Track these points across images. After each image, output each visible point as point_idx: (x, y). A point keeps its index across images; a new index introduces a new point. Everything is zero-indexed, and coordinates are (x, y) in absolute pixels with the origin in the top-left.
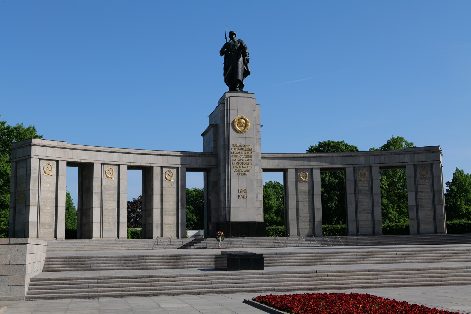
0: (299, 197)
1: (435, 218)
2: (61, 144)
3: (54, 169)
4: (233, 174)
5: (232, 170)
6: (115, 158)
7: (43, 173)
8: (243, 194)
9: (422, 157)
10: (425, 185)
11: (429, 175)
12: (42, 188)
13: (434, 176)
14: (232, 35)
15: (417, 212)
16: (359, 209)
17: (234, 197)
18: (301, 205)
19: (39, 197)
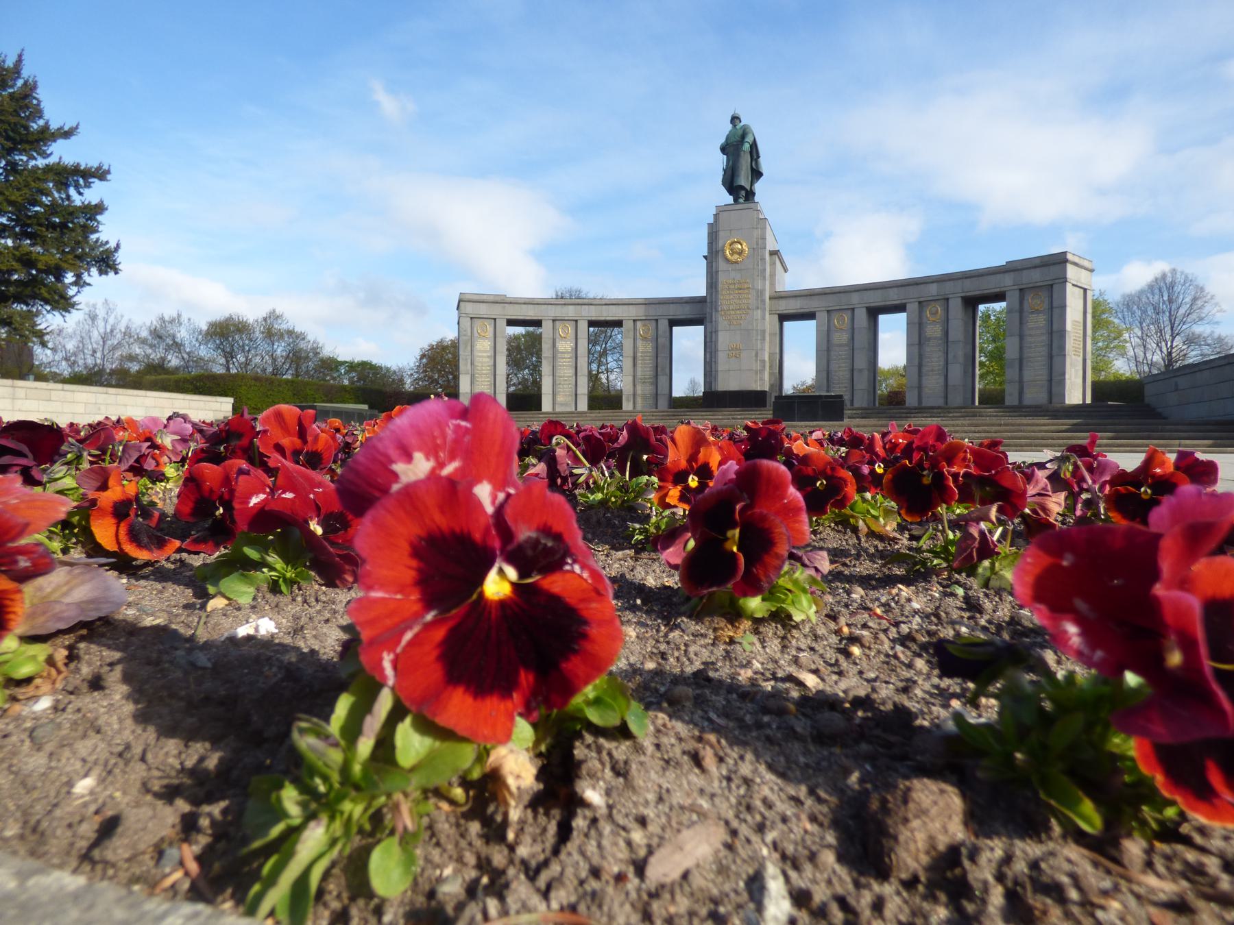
0: (832, 353)
1: (1050, 381)
2: (498, 299)
3: (490, 329)
4: (722, 323)
5: (720, 319)
6: (571, 311)
7: (476, 334)
8: (735, 352)
9: (1036, 276)
10: (1037, 322)
11: (1046, 305)
12: (476, 353)
13: (1055, 304)
14: (735, 119)
15: (1021, 369)
16: (925, 369)
17: (722, 357)
18: (834, 366)
19: (472, 364)
